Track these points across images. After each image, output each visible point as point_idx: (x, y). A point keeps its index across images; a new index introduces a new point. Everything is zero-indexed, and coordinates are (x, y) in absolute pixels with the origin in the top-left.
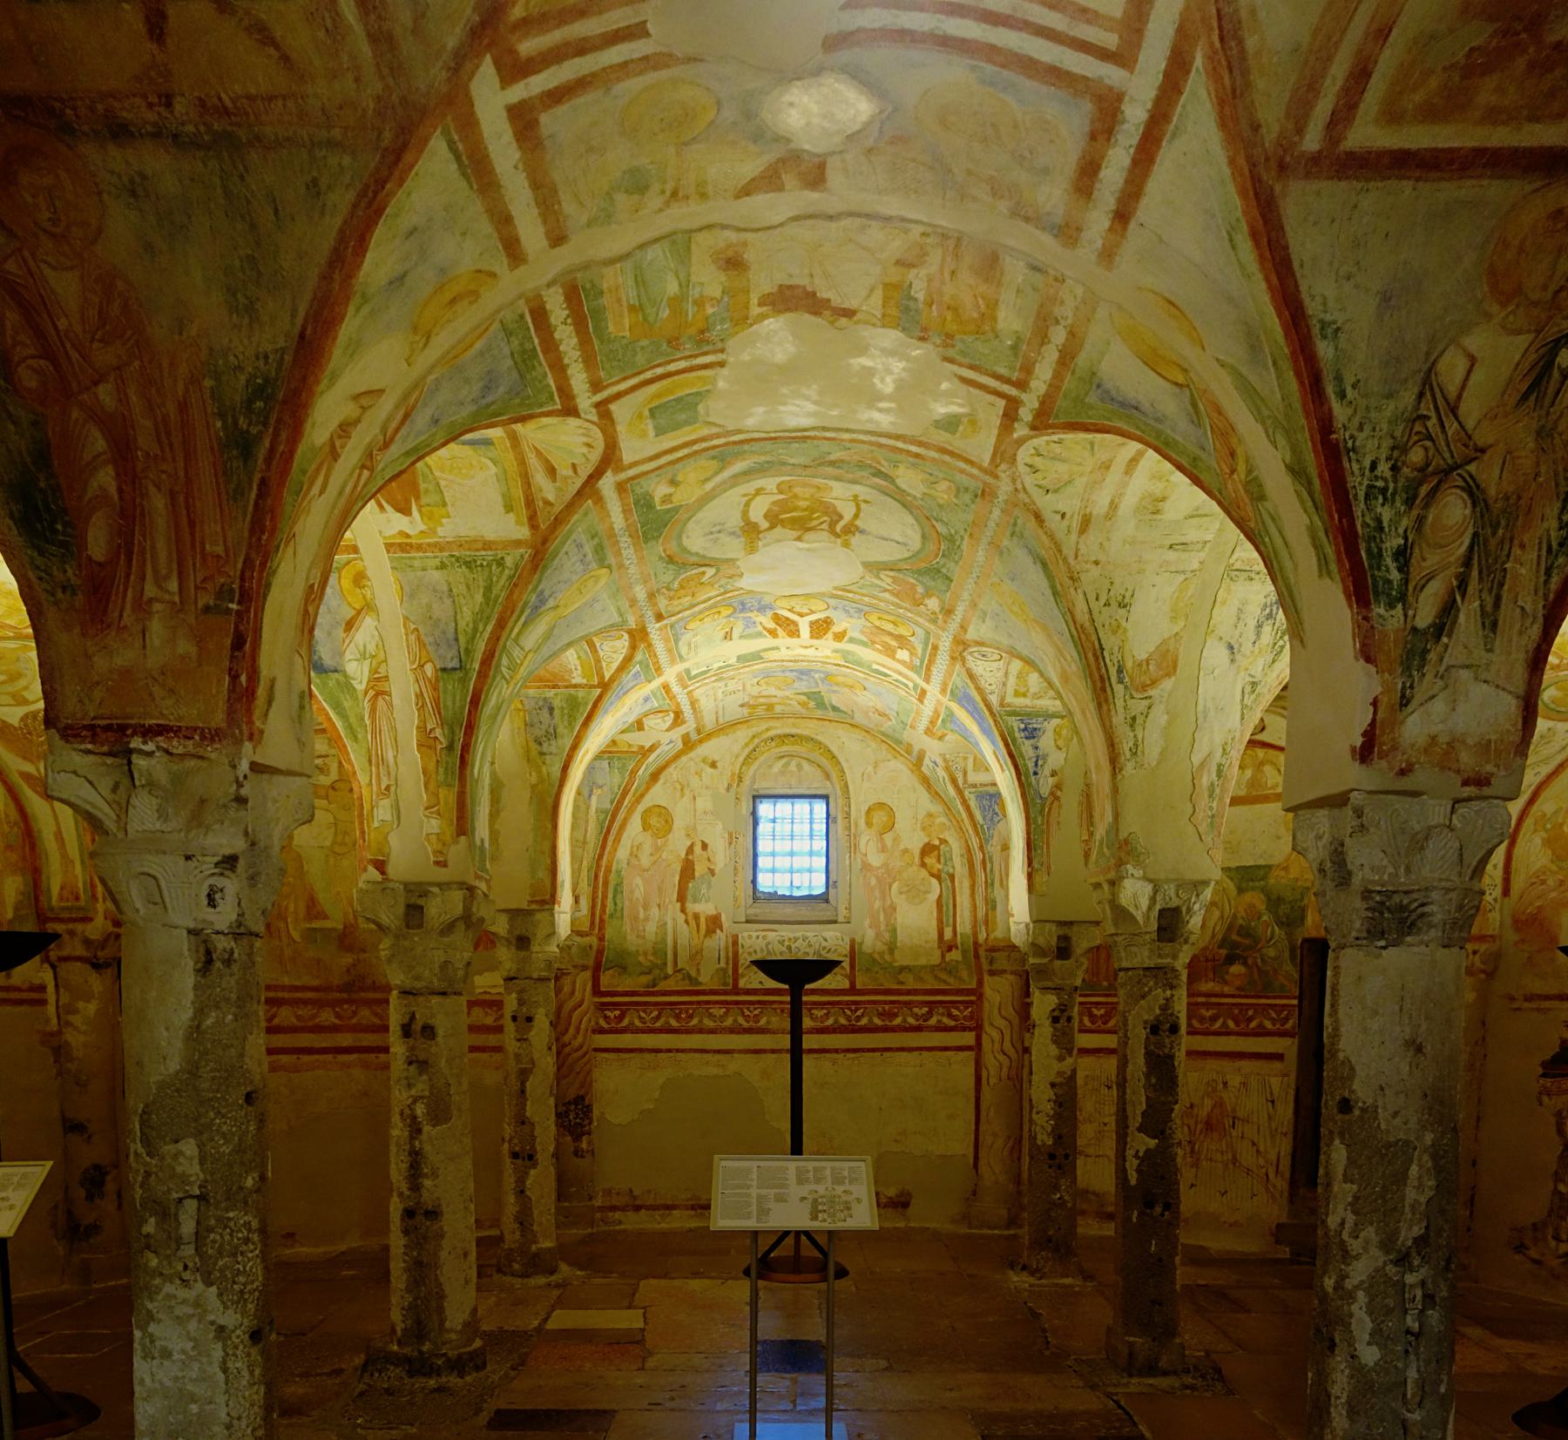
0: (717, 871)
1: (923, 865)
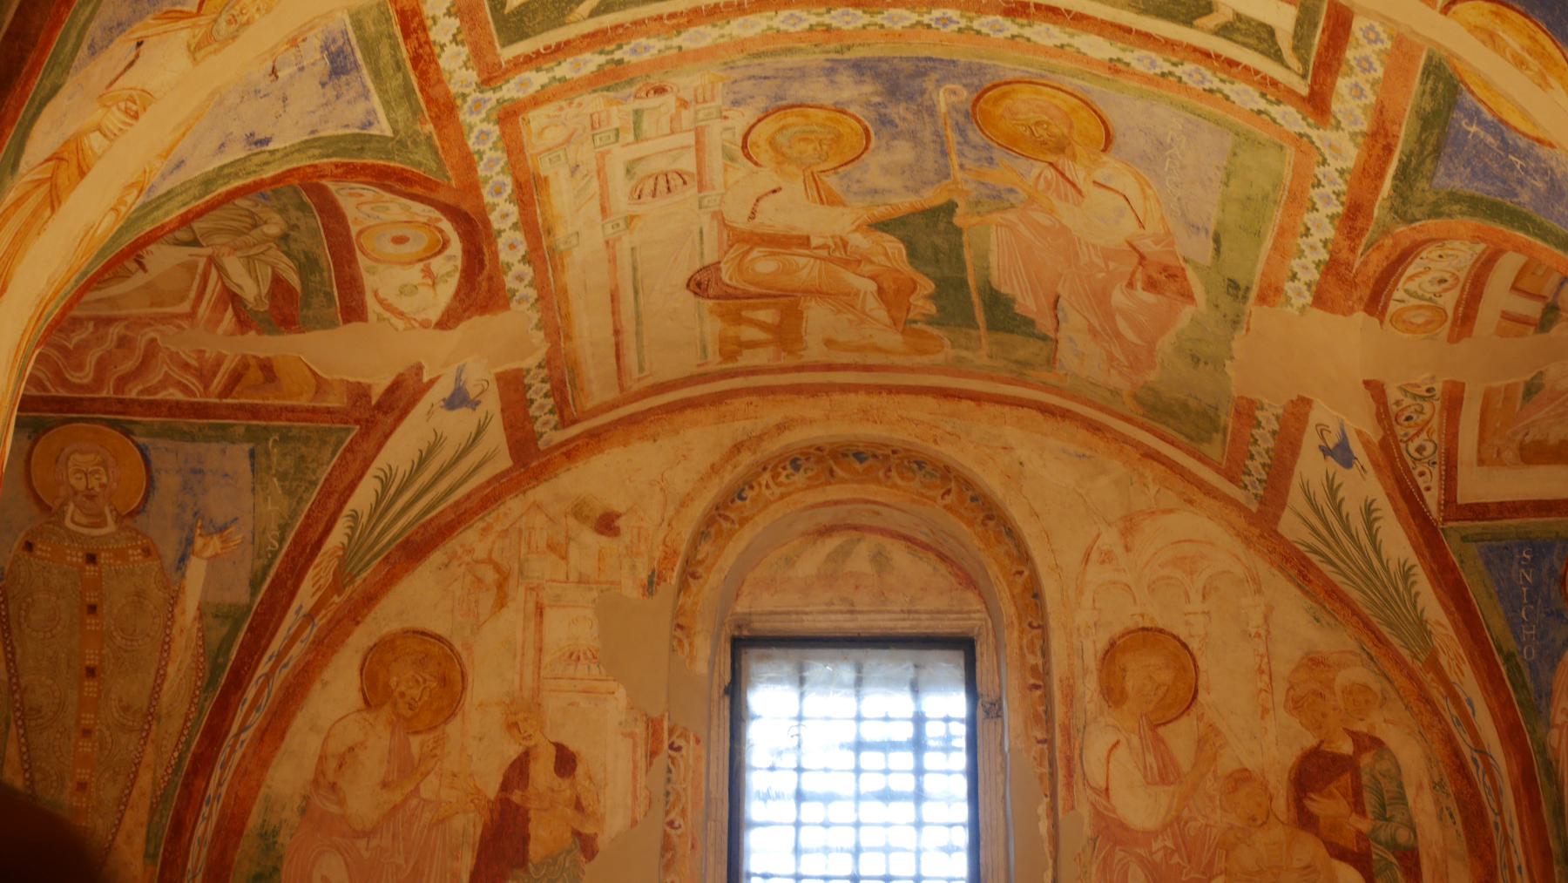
0: (603, 842)
1: (1305, 820)
